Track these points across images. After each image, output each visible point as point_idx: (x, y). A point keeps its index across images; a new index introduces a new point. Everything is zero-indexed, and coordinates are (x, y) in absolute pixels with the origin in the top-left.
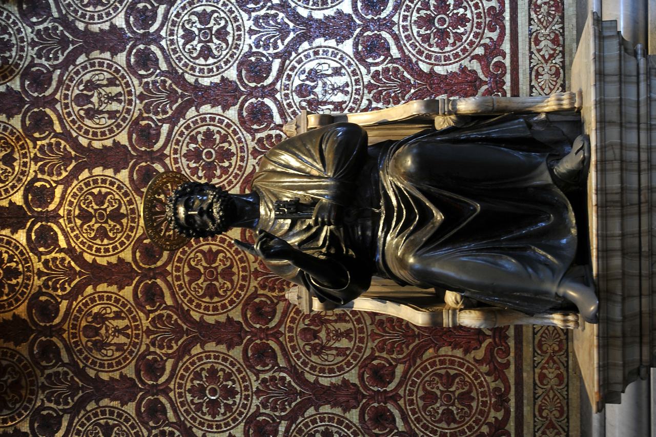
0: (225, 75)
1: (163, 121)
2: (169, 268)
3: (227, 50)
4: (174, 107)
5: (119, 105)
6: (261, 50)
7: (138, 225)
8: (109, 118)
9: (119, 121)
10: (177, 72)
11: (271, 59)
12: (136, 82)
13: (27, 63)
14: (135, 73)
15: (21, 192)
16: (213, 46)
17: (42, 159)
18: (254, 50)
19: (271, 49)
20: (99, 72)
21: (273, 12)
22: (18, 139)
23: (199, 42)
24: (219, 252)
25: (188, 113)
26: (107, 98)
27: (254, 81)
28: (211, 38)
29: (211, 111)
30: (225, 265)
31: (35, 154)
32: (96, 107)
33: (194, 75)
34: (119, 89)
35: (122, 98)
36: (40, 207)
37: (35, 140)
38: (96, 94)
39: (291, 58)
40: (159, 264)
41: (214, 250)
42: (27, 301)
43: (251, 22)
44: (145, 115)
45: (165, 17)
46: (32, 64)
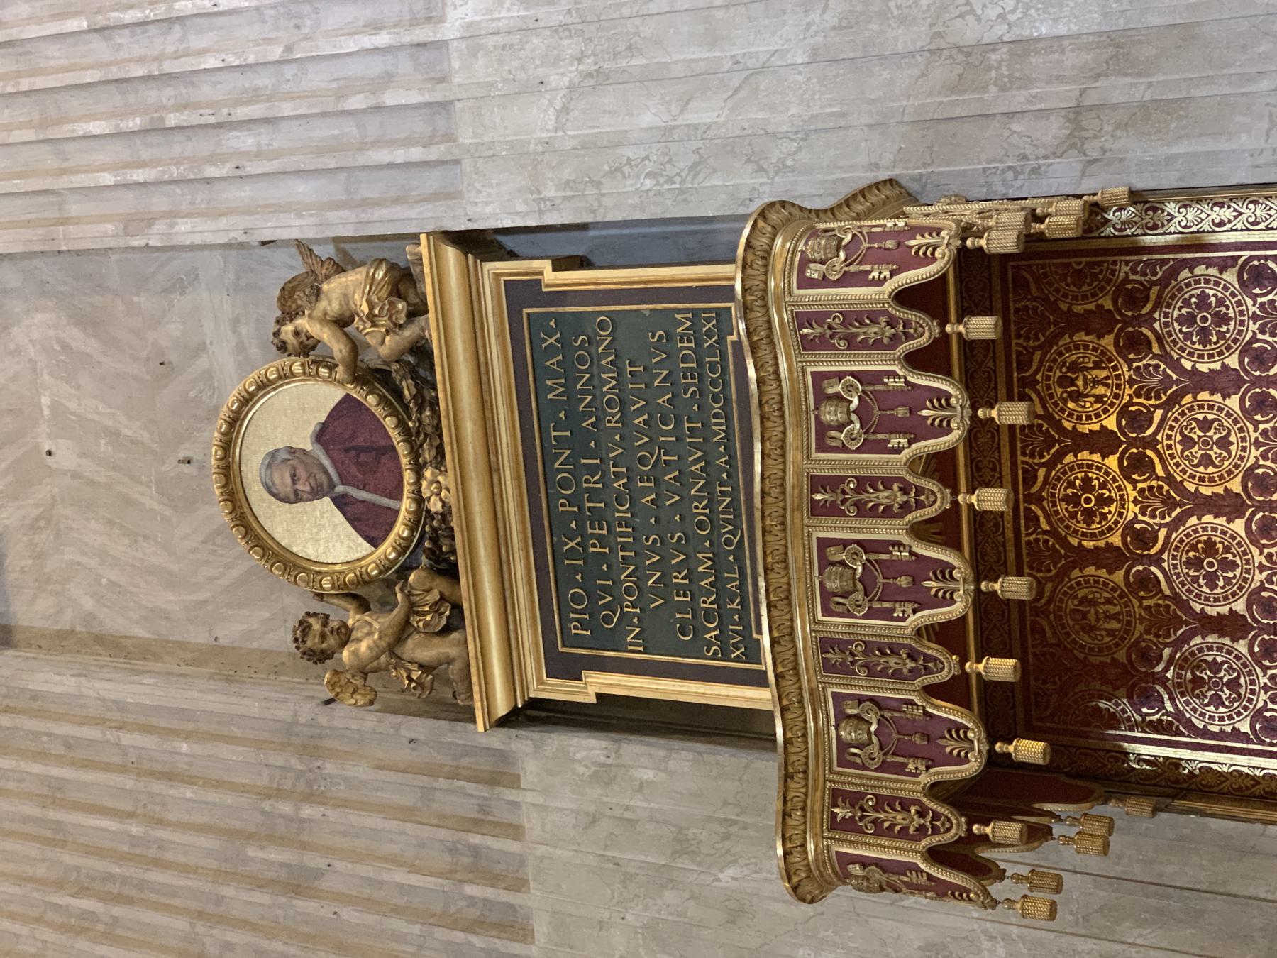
13: (1247, 339)
15: (1239, 478)
17: (1265, 445)
22: (1236, 422)
31: (1257, 438)
36: (1261, 496)
37: (1256, 424)
42: (1246, 596)
46: (1254, 339)
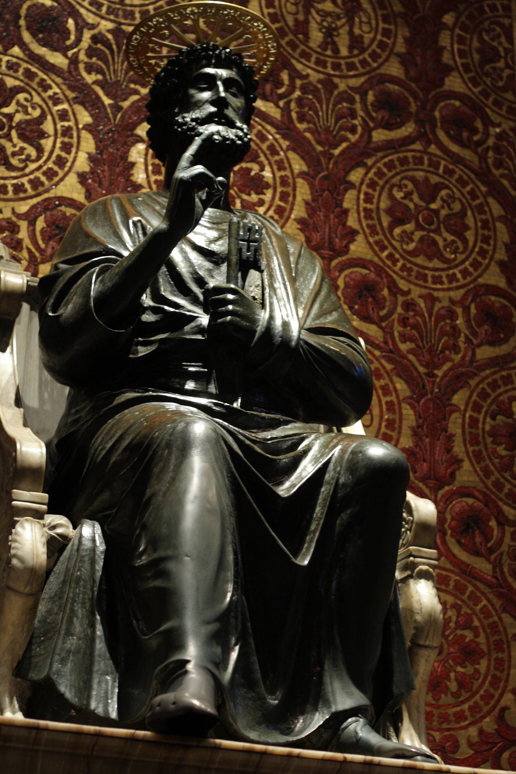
0: (360, 238)
1: (286, 111)
2: (16, 50)
3: (401, 251)
4: (308, 135)
5: (318, 43)
6: (399, 310)
7: (102, 17)
8: (296, 20)
9: (291, 36)
10: (369, 156)
11: (384, 324)
12: (355, 82)
14: (370, 84)
16: (409, 227)
18: (401, 299)
19: (401, 329)
20: (374, 26)
21: (462, 345)
23: (416, 205)
24: (40, 150)
25: (297, 157)
26: (330, 26)
27: (347, 285)
28: (423, 229)
29: (299, 198)
30: (14, 154)
32: (316, 5)
33: (362, 183)
34: (344, 52)
35: (329, 53)
38: (338, 10)
39: (383, 361)
40: (26, 36)
41: (43, 142)
43: (446, 303)
44: (298, 82)
45: (457, 159)
